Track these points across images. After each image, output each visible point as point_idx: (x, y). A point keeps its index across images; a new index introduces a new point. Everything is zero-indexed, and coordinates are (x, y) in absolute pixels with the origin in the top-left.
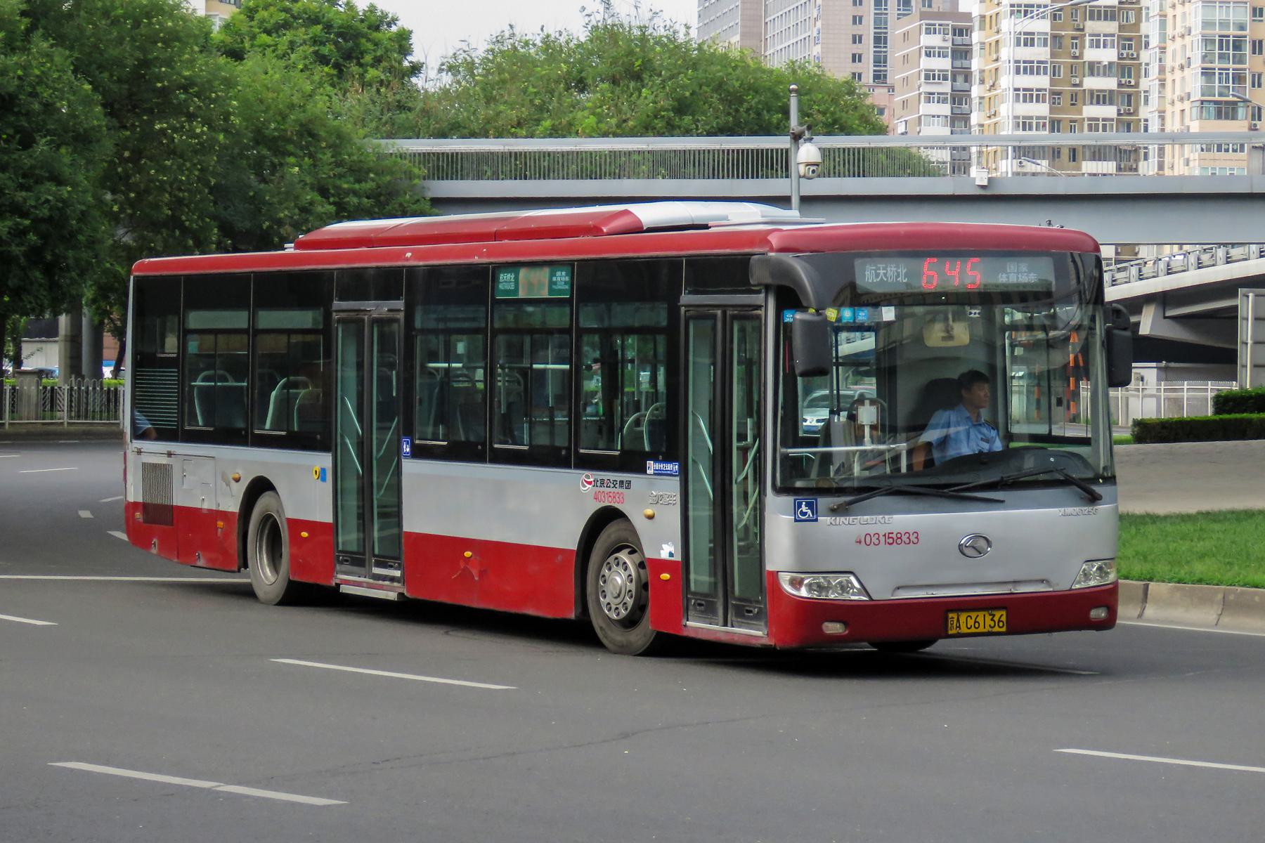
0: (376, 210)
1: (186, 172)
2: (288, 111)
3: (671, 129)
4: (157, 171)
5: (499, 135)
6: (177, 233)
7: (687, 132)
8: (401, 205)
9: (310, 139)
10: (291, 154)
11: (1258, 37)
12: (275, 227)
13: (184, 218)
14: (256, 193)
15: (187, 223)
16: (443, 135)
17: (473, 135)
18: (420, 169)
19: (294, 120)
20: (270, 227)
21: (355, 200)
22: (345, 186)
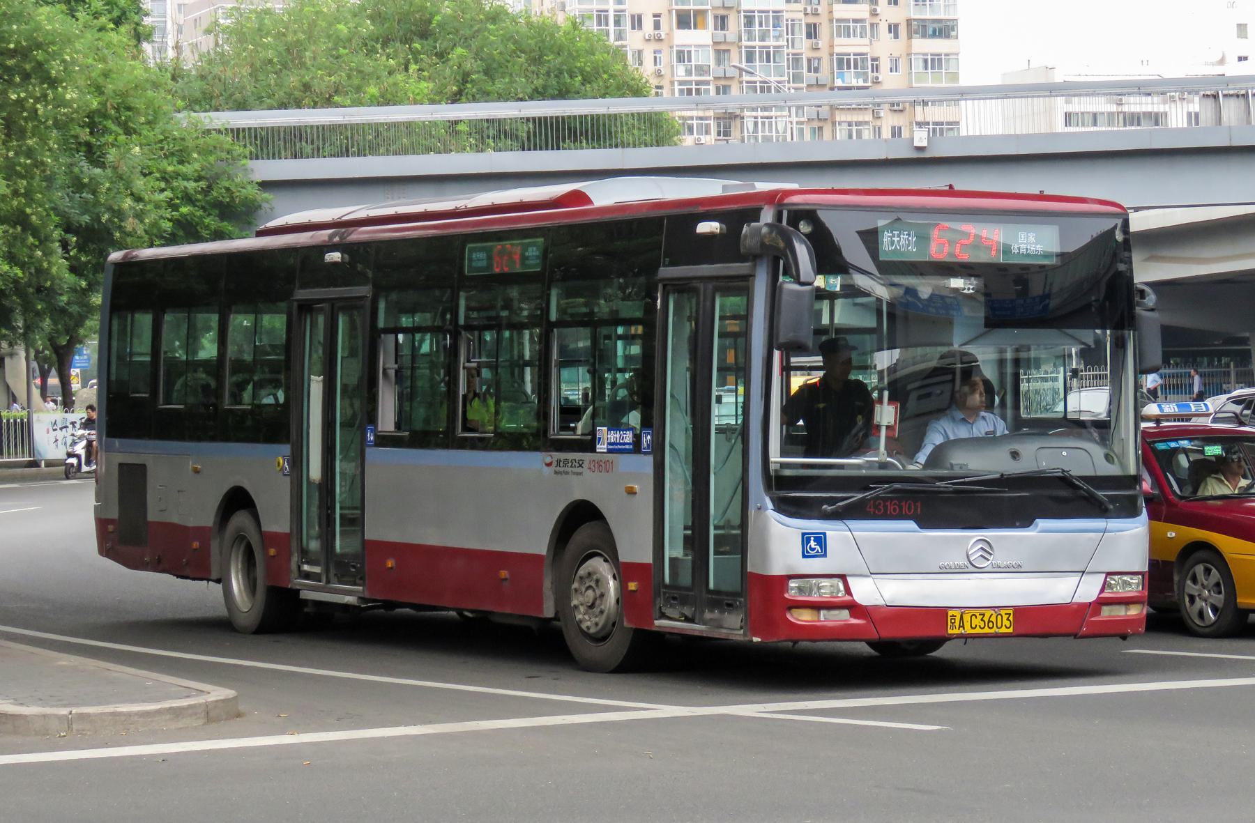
0: (199, 197)
1: (48, 153)
2: (101, 80)
3: (485, 96)
4: (17, 154)
5: (328, 102)
6: (19, 228)
7: (502, 97)
8: (228, 189)
9: (130, 113)
10: (106, 131)
11: (636, 11)
12: (116, 220)
13: (28, 211)
14: (91, 179)
15: (34, 218)
16: (242, 106)
17: (283, 106)
18: (245, 146)
19: (114, 91)
20: (109, 220)
21: (185, 183)
22: (170, 169)
